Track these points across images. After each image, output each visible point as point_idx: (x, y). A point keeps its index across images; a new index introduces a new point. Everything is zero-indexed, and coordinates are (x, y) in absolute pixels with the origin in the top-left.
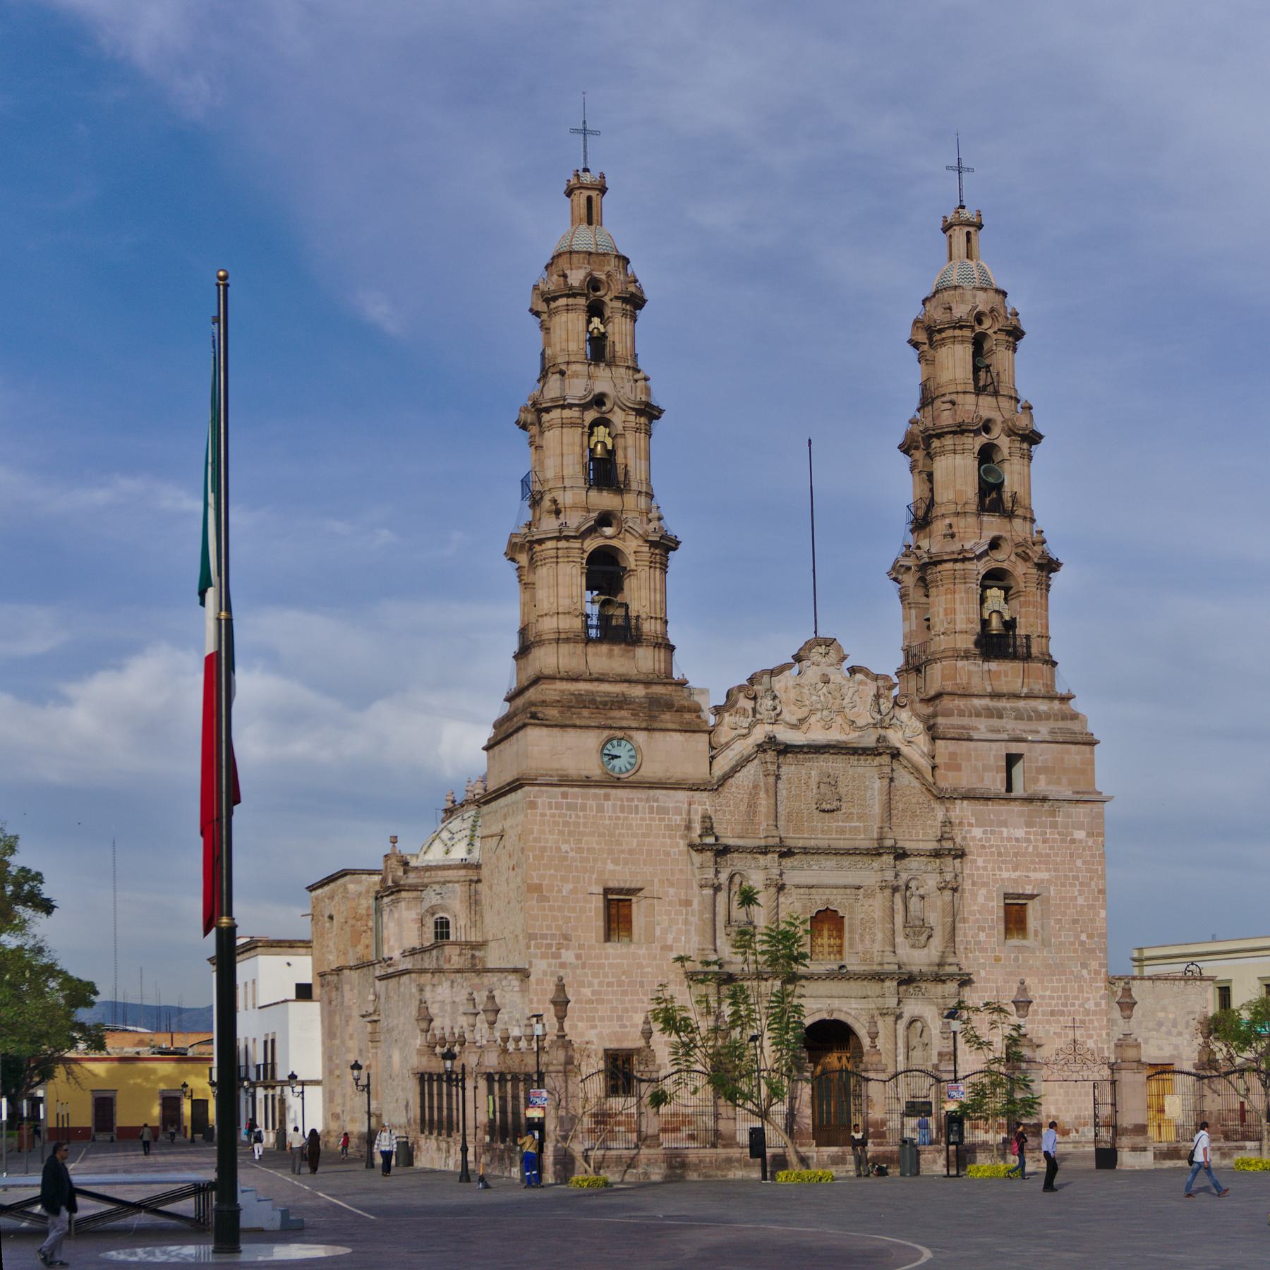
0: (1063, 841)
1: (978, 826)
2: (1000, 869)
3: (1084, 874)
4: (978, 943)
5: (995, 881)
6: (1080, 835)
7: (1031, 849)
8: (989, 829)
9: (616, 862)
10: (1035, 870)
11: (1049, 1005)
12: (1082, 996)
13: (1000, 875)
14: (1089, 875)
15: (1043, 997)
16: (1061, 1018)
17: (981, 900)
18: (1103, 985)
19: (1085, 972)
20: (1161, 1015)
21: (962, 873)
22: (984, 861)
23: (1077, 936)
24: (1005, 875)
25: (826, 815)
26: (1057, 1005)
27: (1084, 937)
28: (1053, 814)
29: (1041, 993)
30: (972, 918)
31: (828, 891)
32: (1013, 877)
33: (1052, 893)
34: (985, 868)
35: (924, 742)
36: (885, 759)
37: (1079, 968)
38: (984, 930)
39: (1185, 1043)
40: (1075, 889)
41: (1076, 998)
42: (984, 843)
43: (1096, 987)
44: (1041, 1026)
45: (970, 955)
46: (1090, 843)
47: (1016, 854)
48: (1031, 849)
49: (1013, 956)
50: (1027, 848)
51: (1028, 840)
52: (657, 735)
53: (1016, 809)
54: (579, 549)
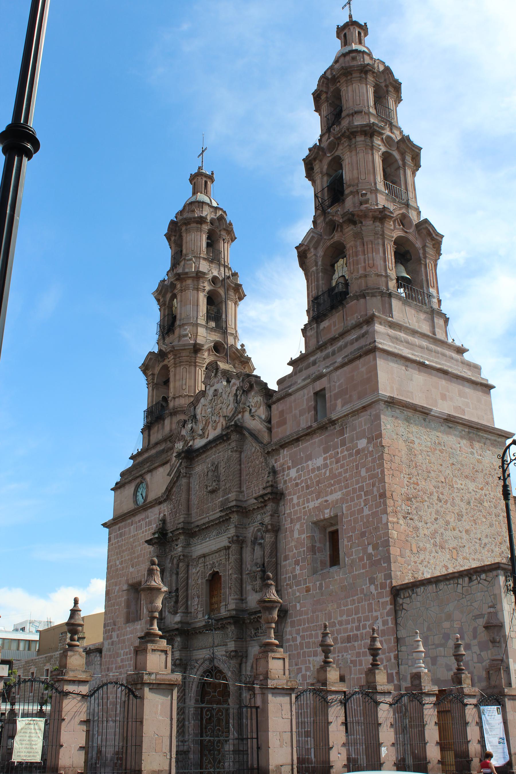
0: (351, 455)
1: (293, 467)
2: (308, 502)
3: (368, 482)
4: (295, 577)
5: (305, 513)
6: (362, 443)
7: (328, 474)
8: (300, 466)
9: (132, 567)
10: (331, 493)
11: (346, 630)
12: (372, 615)
13: (308, 507)
14: (371, 481)
15: (341, 623)
16: (356, 644)
17: (296, 535)
18: (388, 599)
19: (372, 587)
20: (446, 625)
21: (284, 514)
22: (298, 498)
23: (365, 550)
24: (311, 505)
25: (214, 496)
26: (352, 630)
27: (370, 550)
28: (342, 432)
29: (339, 619)
30: (291, 554)
31: (214, 556)
32: (317, 505)
33: (344, 512)
34: (298, 504)
35: (263, 412)
36: (234, 437)
37: (368, 585)
38: (297, 563)
39: (475, 660)
40: (362, 500)
41: (367, 619)
42: (297, 481)
43: (383, 603)
44: (340, 655)
45: (290, 590)
46: (371, 449)
47: (318, 483)
48: (328, 474)
49: (318, 583)
50: (325, 473)
51: (326, 466)
52: (154, 472)
53: (317, 440)
54: (150, 375)
